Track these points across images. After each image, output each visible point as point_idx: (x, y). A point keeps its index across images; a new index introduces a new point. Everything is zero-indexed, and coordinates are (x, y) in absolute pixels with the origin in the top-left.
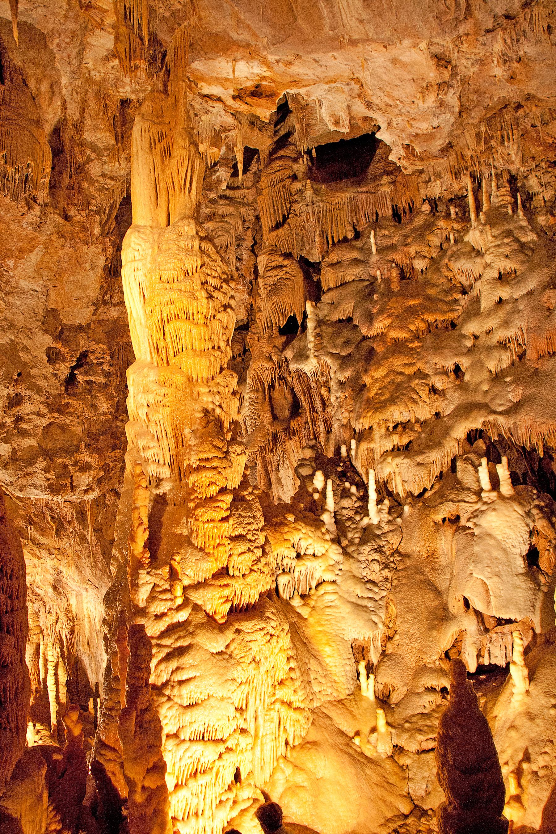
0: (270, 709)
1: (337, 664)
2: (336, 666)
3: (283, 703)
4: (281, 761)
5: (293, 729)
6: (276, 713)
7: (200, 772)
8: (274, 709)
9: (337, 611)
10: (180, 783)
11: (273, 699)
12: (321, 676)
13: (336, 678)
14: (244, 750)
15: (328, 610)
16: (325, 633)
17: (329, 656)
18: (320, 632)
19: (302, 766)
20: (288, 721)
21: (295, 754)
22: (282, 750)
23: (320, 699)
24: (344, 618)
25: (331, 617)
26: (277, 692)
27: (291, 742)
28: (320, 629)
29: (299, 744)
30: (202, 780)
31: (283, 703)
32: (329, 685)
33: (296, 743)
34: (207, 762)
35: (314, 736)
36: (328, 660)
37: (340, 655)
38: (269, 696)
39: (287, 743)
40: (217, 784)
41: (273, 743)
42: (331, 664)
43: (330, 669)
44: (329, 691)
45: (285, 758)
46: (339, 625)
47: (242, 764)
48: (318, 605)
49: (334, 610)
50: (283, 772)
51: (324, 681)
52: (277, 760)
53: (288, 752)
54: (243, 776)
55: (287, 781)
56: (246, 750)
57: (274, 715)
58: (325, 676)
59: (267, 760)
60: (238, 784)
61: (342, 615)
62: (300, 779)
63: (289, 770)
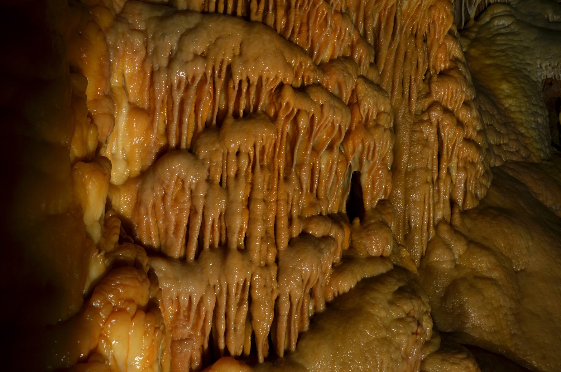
0: (422, 122)
1: (523, 110)
2: (521, 112)
3: (446, 110)
4: (444, 228)
5: (462, 175)
6: (434, 130)
7: (236, 115)
8: (429, 121)
9: (515, 38)
10: (173, 143)
11: (426, 103)
12: (498, 122)
13: (523, 131)
14: (371, 124)
15: (500, 40)
16: (498, 67)
17: (508, 96)
18: (489, 66)
19: (486, 243)
20: (455, 161)
21: (469, 223)
22: (442, 212)
23: (500, 157)
24: (527, 48)
25: (504, 47)
26: (434, 87)
27: (460, 202)
28: (488, 62)
29: (474, 209)
30: (241, 141)
31: (446, 110)
32: (513, 137)
33: (469, 206)
34: (254, 79)
35: (497, 199)
36: (508, 103)
37: (526, 97)
38: (418, 99)
39: (453, 203)
40: (294, 177)
41: (429, 190)
42: (513, 109)
43: (513, 116)
44: (514, 147)
45: (451, 225)
46: (521, 57)
47: (365, 169)
48: (481, 35)
49: (510, 37)
50: (448, 247)
51: (503, 131)
52: (436, 227)
53: (457, 216)
54: (368, 204)
55: (457, 267)
56: (377, 126)
57: (429, 132)
58: (505, 125)
59: (416, 222)
60: (357, 221)
61: (525, 44)
62: (482, 264)
63: (459, 248)
